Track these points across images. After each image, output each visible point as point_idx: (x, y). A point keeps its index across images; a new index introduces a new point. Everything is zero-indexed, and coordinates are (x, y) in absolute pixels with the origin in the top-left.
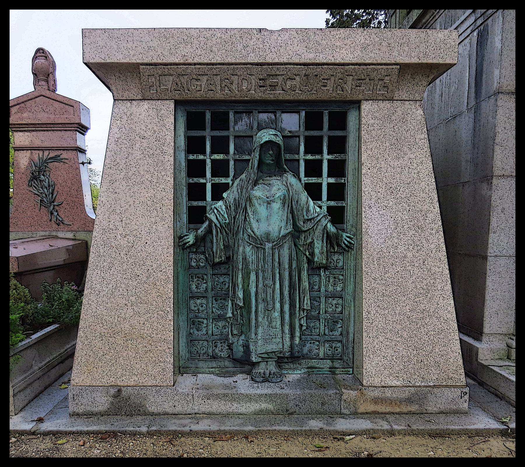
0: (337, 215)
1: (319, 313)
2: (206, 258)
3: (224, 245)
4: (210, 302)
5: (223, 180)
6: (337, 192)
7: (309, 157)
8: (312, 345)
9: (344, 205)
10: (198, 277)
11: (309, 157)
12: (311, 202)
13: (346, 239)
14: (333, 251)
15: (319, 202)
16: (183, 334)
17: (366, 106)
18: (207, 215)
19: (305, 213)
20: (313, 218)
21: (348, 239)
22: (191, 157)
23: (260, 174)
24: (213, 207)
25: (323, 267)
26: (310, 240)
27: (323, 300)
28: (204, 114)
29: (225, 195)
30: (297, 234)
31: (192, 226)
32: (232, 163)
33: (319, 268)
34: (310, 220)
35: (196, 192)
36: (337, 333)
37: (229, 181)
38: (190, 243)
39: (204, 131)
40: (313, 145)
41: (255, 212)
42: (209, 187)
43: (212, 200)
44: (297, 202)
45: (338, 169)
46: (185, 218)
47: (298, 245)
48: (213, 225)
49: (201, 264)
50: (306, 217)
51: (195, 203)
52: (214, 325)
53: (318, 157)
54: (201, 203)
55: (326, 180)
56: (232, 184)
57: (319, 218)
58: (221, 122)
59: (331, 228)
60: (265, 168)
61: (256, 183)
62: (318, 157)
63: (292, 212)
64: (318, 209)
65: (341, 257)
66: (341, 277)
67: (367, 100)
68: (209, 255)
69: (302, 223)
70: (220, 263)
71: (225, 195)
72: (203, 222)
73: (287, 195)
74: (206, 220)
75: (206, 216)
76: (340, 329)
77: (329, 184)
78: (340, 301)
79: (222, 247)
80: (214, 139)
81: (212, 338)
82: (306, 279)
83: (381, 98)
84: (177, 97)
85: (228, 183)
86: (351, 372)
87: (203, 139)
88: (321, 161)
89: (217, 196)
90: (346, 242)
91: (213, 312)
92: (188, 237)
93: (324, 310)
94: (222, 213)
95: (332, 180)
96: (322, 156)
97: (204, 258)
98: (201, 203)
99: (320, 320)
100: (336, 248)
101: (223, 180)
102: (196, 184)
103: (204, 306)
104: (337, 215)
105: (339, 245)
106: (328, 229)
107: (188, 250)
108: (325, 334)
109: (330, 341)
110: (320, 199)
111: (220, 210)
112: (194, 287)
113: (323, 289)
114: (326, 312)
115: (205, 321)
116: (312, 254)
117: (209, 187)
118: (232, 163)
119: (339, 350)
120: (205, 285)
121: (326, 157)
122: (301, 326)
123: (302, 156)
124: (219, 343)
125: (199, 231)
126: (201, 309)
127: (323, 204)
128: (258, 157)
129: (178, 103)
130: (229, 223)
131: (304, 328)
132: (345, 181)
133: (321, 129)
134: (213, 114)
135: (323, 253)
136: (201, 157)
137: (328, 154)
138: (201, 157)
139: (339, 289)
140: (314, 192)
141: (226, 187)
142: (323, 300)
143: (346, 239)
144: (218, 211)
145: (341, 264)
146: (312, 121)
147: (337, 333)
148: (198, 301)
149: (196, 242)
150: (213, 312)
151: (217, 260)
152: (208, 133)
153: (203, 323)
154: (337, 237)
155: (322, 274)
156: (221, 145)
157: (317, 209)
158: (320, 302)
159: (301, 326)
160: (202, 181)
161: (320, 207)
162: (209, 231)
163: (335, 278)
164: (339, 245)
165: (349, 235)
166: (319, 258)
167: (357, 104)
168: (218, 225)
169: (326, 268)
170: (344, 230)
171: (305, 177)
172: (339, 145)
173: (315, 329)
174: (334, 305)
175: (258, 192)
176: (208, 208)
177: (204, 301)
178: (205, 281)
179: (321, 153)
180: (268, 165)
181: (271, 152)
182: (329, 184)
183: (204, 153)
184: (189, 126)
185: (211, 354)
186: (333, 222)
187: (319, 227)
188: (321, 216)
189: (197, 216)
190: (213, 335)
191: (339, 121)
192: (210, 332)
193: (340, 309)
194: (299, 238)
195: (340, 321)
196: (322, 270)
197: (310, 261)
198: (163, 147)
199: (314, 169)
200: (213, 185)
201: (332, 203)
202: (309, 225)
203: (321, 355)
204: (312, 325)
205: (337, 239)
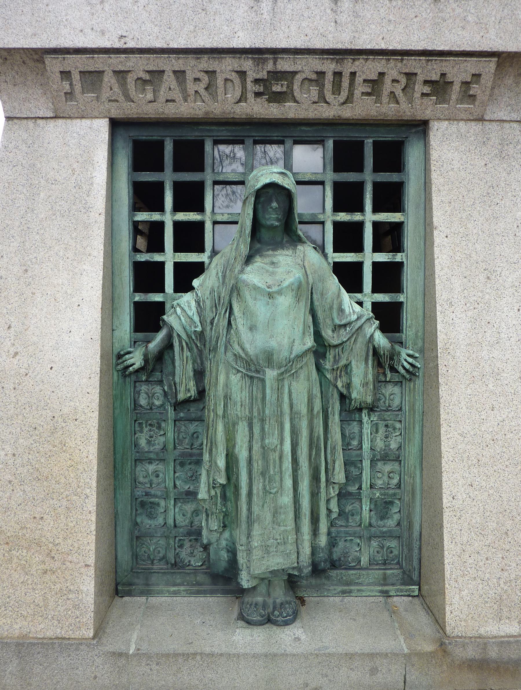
0: (389, 317)
1: (360, 488)
2: (164, 390)
3: (195, 371)
4: (171, 468)
6: (389, 277)
8: (348, 544)
9: (402, 300)
10: (150, 425)
12: (345, 295)
13: (406, 360)
14: (384, 379)
15: (359, 296)
16: (125, 525)
17: (438, 131)
18: (165, 317)
19: (335, 315)
20: (350, 323)
21: (410, 360)
23: (258, 246)
24: (175, 303)
25: (366, 408)
26: (343, 362)
27: (366, 464)
28: (161, 144)
29: (196, 283)
30: (321, 350)
31: (140, 335)
33: (360, 410)
34: (345, 326)
35: (147, 277)
36: (391, 523)
38: (136, 367)
39: (162, 173)
40: (347, 198)
41: (246, 312)
43: (176, 291)
44: (322, 294)
45: (390, 237)
47: (324, 371)
48: (175, 335)
49: (157, 403)
50: (337, 322)
52: (177, 510)
55: (369, 258)
56: (210, 264)
57: (359, 323)
59: (381, 340)
60: (265, 234)
61: (249, 260)
63: (313, 312)
64: (357, 308)
65: (397, 390)
66: (398, 425)
67: (439, 119)
68: (170, 386)
69: (330, 332)
70: (187, 401)
71: (196, 283)
72: (157, 329)
73: (303, 282)
74: (164, 325)
75: (163, 320)
76: (396, 517)
77: (375, 265)
78: (396, 466)
79: (191, 374)
80: (177, 186)
81: (173, 532)
82: (338, 430)
83: (463, 116)
84: (115, 113)
85: (203, 263)
86: (416, 593)
87: (160, 186)
89: (183, 284)
90: (405, 364)
91: (175, 486)
92: (131, 355)
93: (369, 484)
94: (190, 314)
95: (382, 257)
96: (364, 215)
97: (161, 392)
99: (361, 500)
100: (389, 375)
102: (147, 263)
103: (161, 475)
104: (389, 317)
105: (393, 369)
106: (375, 343)
107: (133, 378)
108: (370, 525)
109: (379, 537)
110: (360, 290)
111: (186, 308)
112: (143, 442)
113: (366, 446)
114: (371, 487)
115: (163, 503)
116: (348, 386)
119: (396, 552)
120: (162, 439)
121: (369, 217)
122: (329, 511)
124: (187, 541)
125: (152, 346)
126: (155, 480)
127: (365, 299)
128: (252, 214)
129: (116, 125)
130: (202, 332)
131: (334, 516)
132: (402, 259)
134: (177, 144)
135: (367, 383)
139: (394, 446)
140: (349, 277)
141: (198, 269)
142: (366, 464)
143: (406, 360)
144: (183, 311)
145: (396, 402)
146: (346, 157)
147: (391, 523)
148: (151, 468)
149: (145, 365)
150: (175, 486)
151: (181, 396)
152: (168, 178)
153: (158, 504)
154: (393, 355)
155: (365, 419)
156: (190, 197)
157: (355, 308)
158: (362, 469)
159: (329, 511)
161: (360, 304)
163: (387, 426)
164: (393, 369)
165: (411, 352)
166: (359, 393)
167: (421, 127)
168: (184, 336)
169: (371, 409)
170: (402, 343)
171: (334, 251)
172: (390, 197)
173: (353, 515)
174: (386, 475)
175: (254, 275)
176: (167, 306)
177: (161, 467)
178: (162, 433)
180: (272, 228)
181: (275, 205)
183: (161, 209)
184: (137, 166)
185: (173, 562)
186: (383, 329)
187: (360, 339)
188: (363, 320)
189: (148, 318)
190: (175, 526)
191: (391, 157)
192: (171, 522)
193: (395, 481)
194: (324, 356)
195: (397, 502)
196: (365, 412)
197: (343, 397)
198: (87, 199)
199: (348, 237)
200: (176, 264)
201: (382, 298)
202: (344, 335)
203: (364, 560)
204: (349, 508)
205: (392, 359)
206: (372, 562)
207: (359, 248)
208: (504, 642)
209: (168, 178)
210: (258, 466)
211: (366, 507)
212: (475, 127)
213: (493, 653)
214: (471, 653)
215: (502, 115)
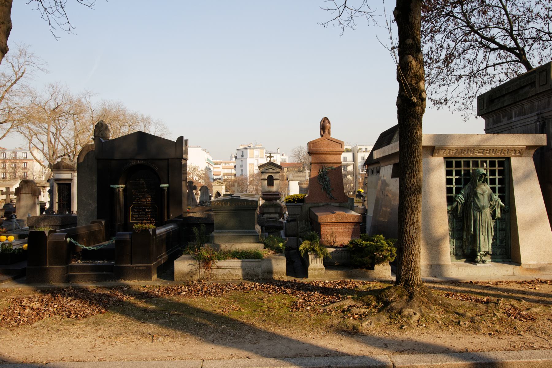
5: (460, 186)
7: (491, 177)
11: (491, 177)
22: (448, 177)
32: (463, 180)
36: (503, 245)
37: (462, 186)
51: (449, 195)
55: (497, 186)
58: (458, 164)
80: (456, 171)
87: (452, 171)
95: (500, 186)
101: (460, 186)
118: (463, 180)
121: (497, 177)
129: (444, 158)
133: (495, 167)
136: (451, 177)
137: (498, 175)
138: (451, 177)
152: (454, 169)
160: (452, 186)
162: (457, 206)
184: (447, 166)
199: (493, 182)
203: (498, 253)
206: (500, 254)
208: (533, 265)
209: (454, 169)
210: (481, 229)
212: (520, 158)
213: (531, 267)
214: (527, 267)
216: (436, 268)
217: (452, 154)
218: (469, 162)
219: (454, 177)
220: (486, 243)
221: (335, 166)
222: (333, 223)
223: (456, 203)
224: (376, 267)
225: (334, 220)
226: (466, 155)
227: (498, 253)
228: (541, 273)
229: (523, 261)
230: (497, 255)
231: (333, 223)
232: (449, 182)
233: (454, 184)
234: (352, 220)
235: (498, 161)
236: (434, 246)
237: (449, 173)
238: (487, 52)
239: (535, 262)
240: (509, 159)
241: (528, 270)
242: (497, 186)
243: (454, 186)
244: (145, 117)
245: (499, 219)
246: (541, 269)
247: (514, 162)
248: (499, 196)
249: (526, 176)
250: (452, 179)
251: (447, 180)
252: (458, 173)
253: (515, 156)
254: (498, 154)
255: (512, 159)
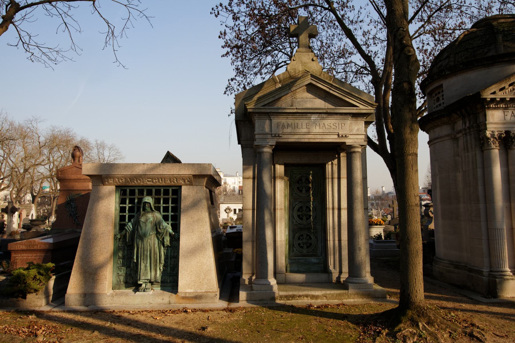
5: (132, 214)
7: (164, 205)
11: (164, 205)
22: (121, 205)
27: (169, 259)
32: (136, 207)
37: (134, 214)
40: (166, 201)
41: (140, 226)
42: (127, 216)
46: (118, 228)
53: (167, 205)
54: (124, 223)
55: (170, 214)
58: (132, 192)
62: (167, 205)
88: (168, 207)
98: (124, 223)
101: (132, 214)
117: (127, 216)
118: (136, 207)
121: (170, 205)
123: (162, 205)
129: (116, 186)
136: (124, 205)
137: (172, 203)
138: (124, 205)
142: (169, 259)
160: (125, 214)
161: (168, 224)
179: (169, 204)
182: (172, 215)
183: (126, 204)
199: (166, 209)
206: (170, 282)
207: (168, 212)
208: (190, 293)
210: (142, 257)
211: (169, 269)
212: (191, 187)
213: (187, 295)
214: (183, 295)
215: (197, 184)
216: (89, 296)
217: (122, 182)
218: (143, 190)
219: (127, 206)
220: (150, 271)
221: (83, 193)
222: (23, 251)
223: (124, 231)
224: (29, 296)
225: (24, 248)
226: (135, 183)
227: (169, 281)
228: (198, 301)
229: (180, 289)
230: (167, 283)
231: (23, 251)
232: (122, 210)
233: (127, 212)
234: (43, 247)
235: (172, 190)
236: (91, 275)
237: (123, 201)
238: (248, 84)
239: (192, 291)
240: (180, 187)
241: (184, 298)
242: (170, 214)
243: (127, 214)
244: (99, 142)
245: (168, 247)
246: (197, 297)
247: (185, 191)
248: (172, 225)
249: (195, 205)
250: (125, 207)
251: (121, 208)
252: (132, 201)
253: (186, 185)
254: (168, 183)
255: (183, 188)
